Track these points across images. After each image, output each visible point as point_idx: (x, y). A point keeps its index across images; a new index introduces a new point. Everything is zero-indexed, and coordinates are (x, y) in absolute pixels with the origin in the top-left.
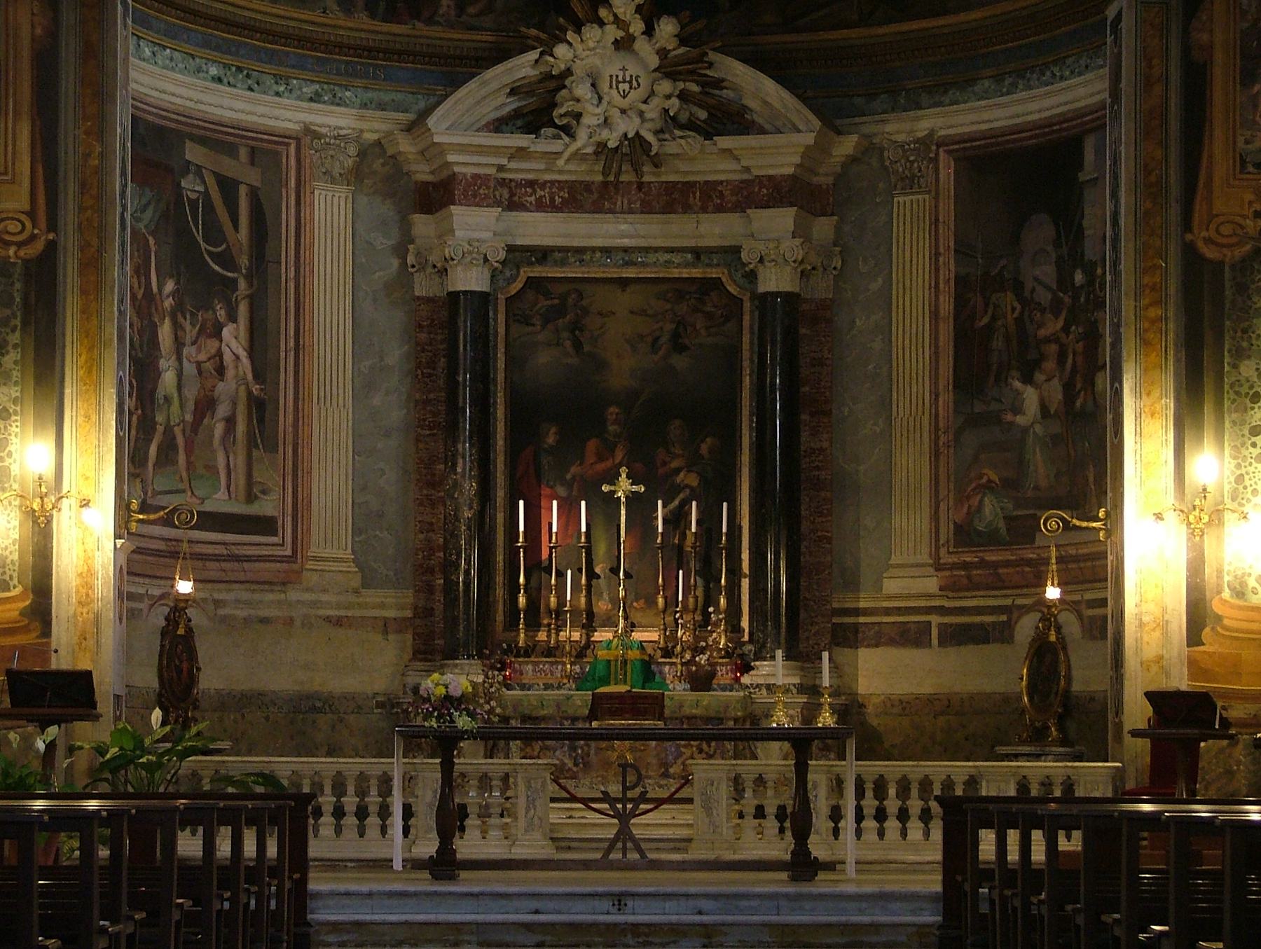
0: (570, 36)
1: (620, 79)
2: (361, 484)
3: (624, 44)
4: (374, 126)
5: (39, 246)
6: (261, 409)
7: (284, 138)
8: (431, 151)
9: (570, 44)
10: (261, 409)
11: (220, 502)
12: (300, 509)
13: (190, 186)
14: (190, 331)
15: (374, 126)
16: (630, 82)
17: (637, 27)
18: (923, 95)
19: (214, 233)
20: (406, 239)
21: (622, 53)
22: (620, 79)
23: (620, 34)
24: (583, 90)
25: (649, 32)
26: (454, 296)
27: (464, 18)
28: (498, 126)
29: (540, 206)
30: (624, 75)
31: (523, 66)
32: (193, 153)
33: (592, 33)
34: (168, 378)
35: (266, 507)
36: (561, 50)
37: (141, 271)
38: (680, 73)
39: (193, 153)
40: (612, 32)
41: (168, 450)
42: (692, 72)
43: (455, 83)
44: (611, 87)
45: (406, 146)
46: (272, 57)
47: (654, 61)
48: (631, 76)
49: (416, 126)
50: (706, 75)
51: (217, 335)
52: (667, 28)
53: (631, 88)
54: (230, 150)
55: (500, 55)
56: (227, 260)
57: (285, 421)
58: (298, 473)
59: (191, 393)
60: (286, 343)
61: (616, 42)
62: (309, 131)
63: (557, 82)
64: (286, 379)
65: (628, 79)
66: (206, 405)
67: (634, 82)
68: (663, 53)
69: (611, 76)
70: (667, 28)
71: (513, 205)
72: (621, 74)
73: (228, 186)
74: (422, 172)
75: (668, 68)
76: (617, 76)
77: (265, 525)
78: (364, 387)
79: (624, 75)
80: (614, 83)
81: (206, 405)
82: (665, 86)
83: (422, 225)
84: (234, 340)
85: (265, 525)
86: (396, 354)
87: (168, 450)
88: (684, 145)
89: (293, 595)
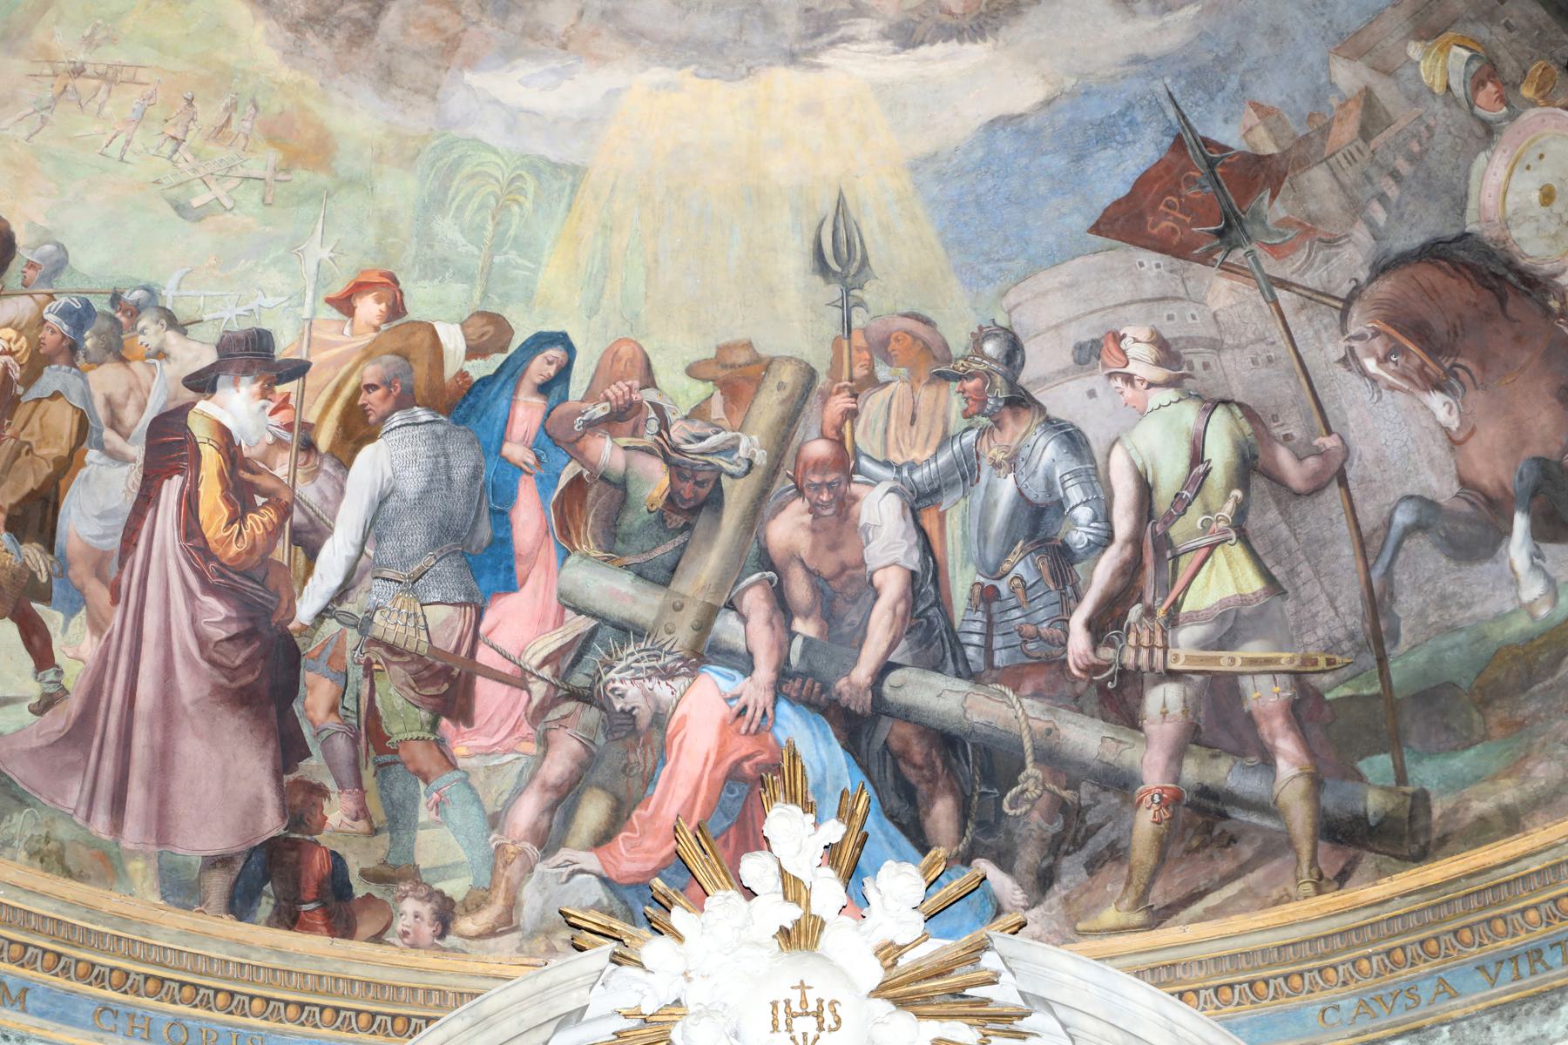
0: (679, 917)
1: (796, 1008)
9: (679, 937)
16: (818, 1015)
17: (827, 891)
18: (1496, 1027)
21: (797, 955)
22: (796, 1008)
23: (790, 914)
25: (857, 903)
27: (451, 940)
30: (804, 1002)
33: (723, 901)
36: (654, 949)
38: (927, 1000)
42: (956, 994)
44: (775, 1028)
47: (874, 974)
48: (820, 1001)
50: (985, 1002)
53: (821, 1029)
61: (784, 933)
65: (813, 1007)
67: (827, 1015)
68: (889, 953)
69: (774, 1005)
72: (795, 997)
76: (788, 1002)
79: (804, 1002)
80: (782, 1017)
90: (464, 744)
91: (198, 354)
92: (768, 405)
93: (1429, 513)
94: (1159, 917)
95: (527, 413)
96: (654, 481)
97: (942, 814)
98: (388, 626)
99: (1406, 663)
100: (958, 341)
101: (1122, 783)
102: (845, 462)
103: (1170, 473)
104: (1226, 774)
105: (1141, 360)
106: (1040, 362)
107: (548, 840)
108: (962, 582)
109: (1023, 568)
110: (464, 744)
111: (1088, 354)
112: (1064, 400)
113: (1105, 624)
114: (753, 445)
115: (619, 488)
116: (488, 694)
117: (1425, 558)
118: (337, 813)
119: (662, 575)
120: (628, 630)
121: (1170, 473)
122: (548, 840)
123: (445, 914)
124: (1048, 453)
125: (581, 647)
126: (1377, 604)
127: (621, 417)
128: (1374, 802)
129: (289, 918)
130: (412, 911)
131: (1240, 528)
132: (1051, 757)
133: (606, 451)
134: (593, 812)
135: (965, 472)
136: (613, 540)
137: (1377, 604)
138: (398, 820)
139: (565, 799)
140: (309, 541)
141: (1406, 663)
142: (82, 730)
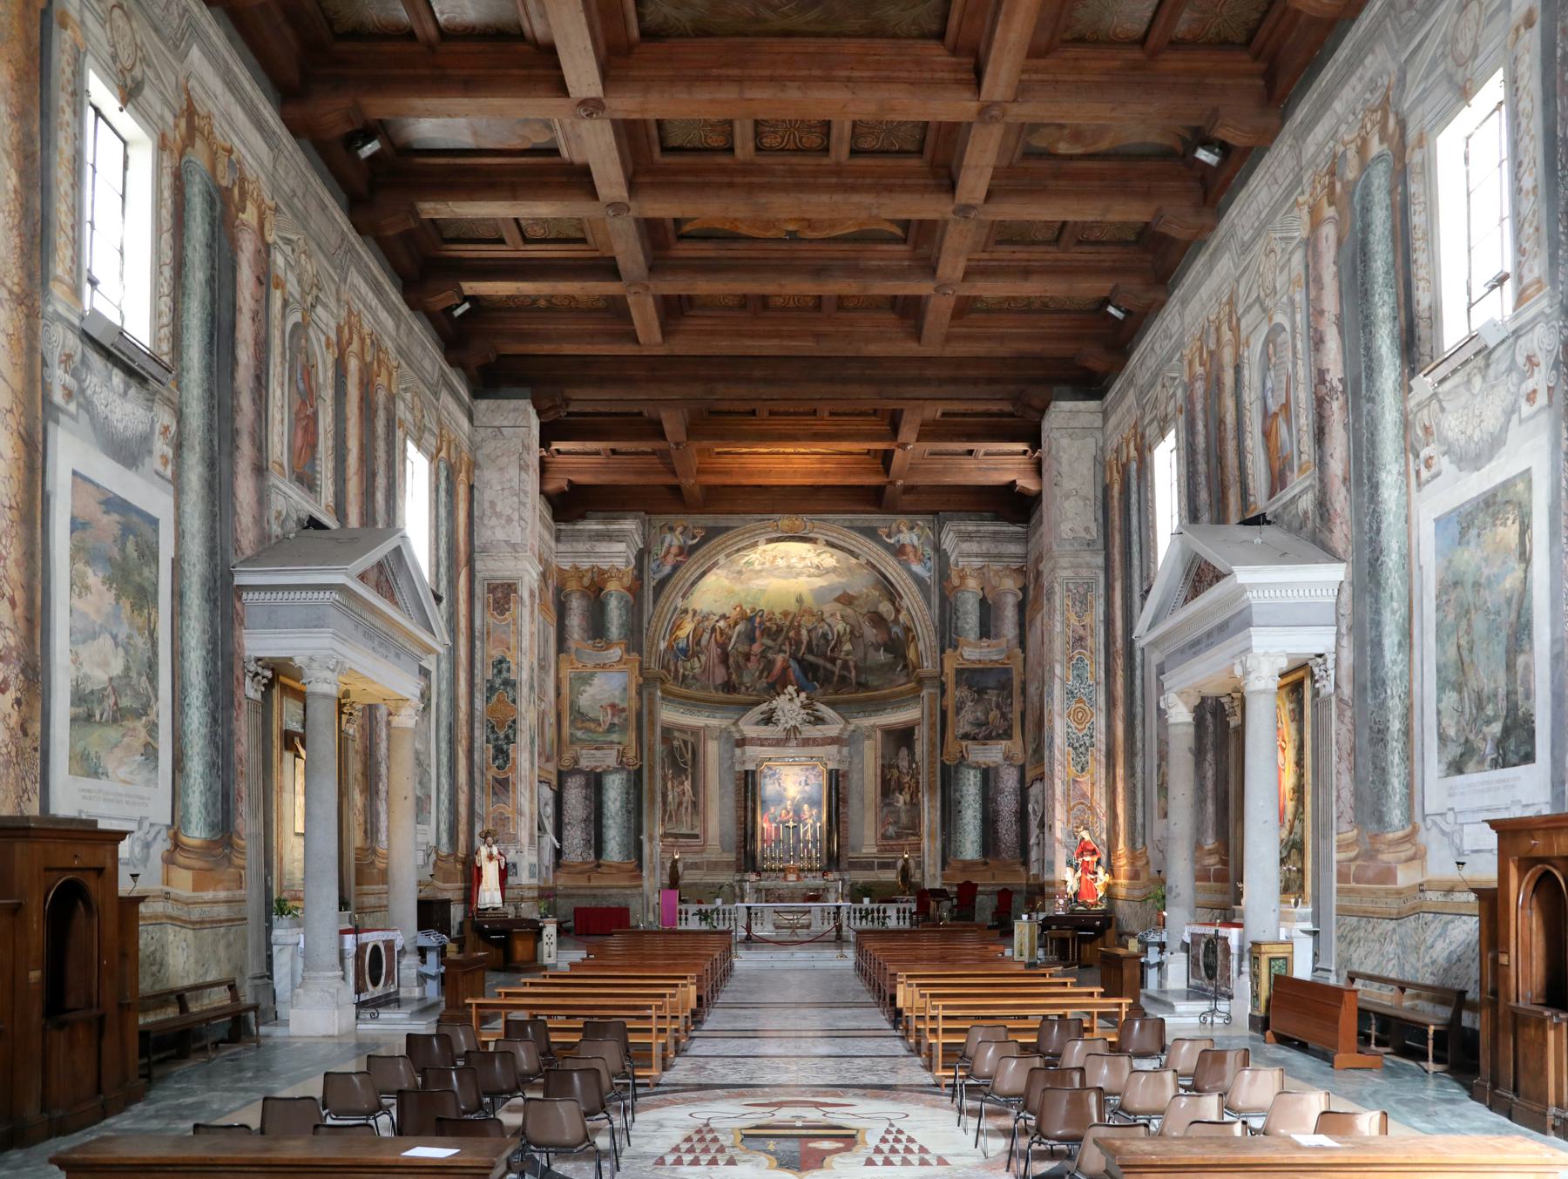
2: (721, 824)
3: (791, 700)
4: (725, 723)
5: (636, 767)
6: (695, 804)
7: (699, 728)
8: (740, 731)
10: (695, 804)
11: (684, 831)
12: (705, 831)
13: (676, 743)
14: (676, 783)
15: (725, 723)
17: (795, 695)
19: (682, 756)
20: (733, 755)
24: (780, 713)
26: (746, 772)
28: (757, 723)
29: (769, 745)
31: (764, 707)
32: (676, 734)
33: (782, 696)
34: (670, 797)
35: (696, 831)
37: (663, 768)
39: (676, 734)
40: (788, 697)
41: (671, 816)
43: (746, 710)
45: (733, 729)
46: (696, 706)
49: (735, 723)
51: (682, 783)
52: (803, 695)
54: (686, 732)
55: (758, 703)
56: (685, 763)
57: (701, 807)
58: (705, 821)
59: (676, 801)
60: (701, 785)
62: (707, 726)
63: (773, 711)
64: (701, 795)
66: (680, 804)
70: (803, 695)
71: (762, 745)
73: (685, 742)
74: (737, 736)
75: (804, 707)
77: (696, 836)
78: (722, 797)
81: (680, 804)
82: (803, 711)
83: (738, 751)
84: (687, 785)
85: (696, 836)
86: (731, 788)
87: (671, 816)
88: (810, 727)
89: (704, 855)
90: (749, 665)
91: (716, 618)
92: (790, 618)
93: (872, 644)
94: (836, 693)
95: (758, 620)
96: (774, 627)
97: (810, 675)
98: (740, 649)
99: (868, 663)
100: (815, 610)
101: (833, 673)
102: (799, 626)
103: (842, 632)
104: (846, 673)
105: (839, 617)
106: (826, 615)
107: (760, 677)
108: (814, 643)
109: (822, 641)
110: (749, 665)
111: (832, 615)
112: (828, 621)
113: (832, 650)
114: (787, 623)
115: (769, 629)
116: (752, 658)
117: (871, 651)
118: (734, 676)
119: (775, 640)
120: (770, 648)
121: (842, 632)
122: (760, 677)
123: (747, 688)
124: (826, 627)
125: (763, 651)
126: (866, 654)
127: (770, 620)
128: (863, 681)
129: (728, 693)
130: (743, 688)
131: (850, 640)
132: (825, 668)
133: (768, 624)
134: (765, 674)
135: (815, 628)
136: (769, 636)
137: (866, 654)
138: (740, 676)
139: (762, 672)
140: (730, 639)
141: (868, 663)
142: (704, 671)
